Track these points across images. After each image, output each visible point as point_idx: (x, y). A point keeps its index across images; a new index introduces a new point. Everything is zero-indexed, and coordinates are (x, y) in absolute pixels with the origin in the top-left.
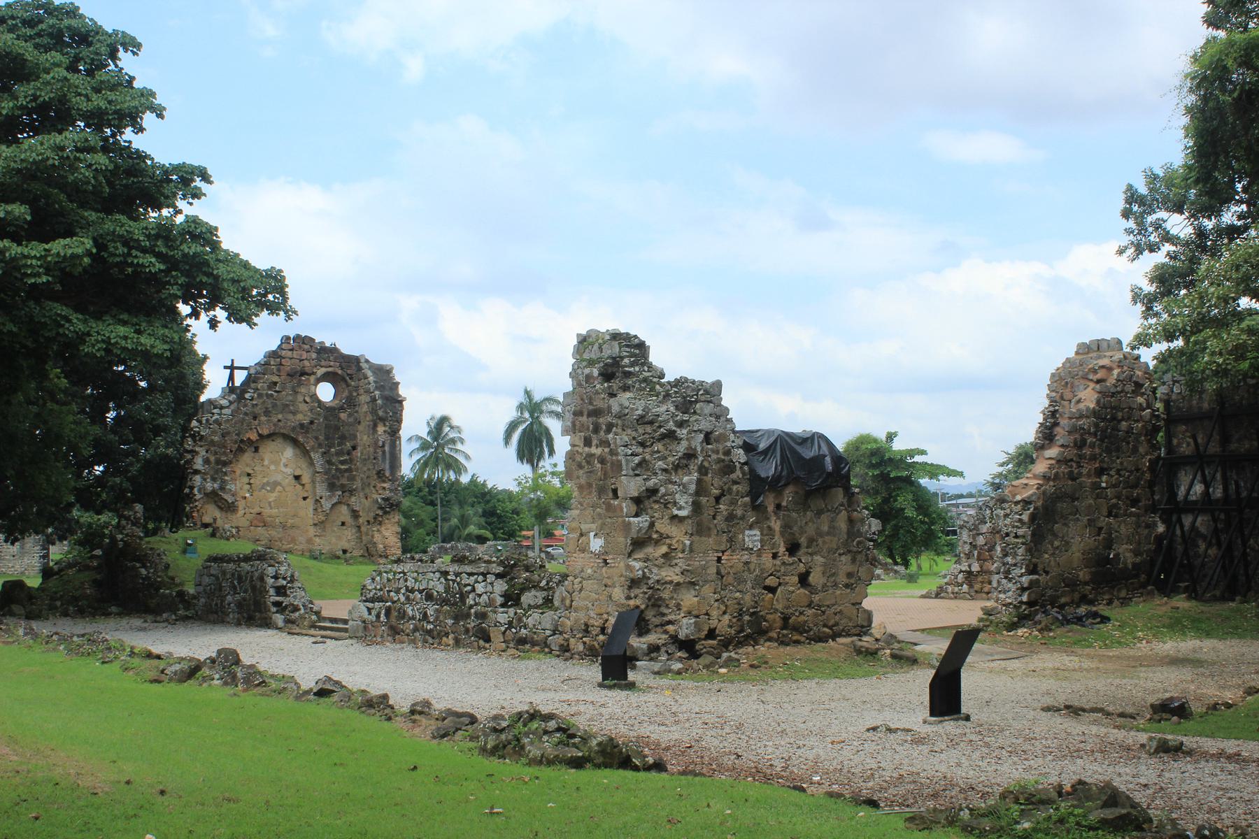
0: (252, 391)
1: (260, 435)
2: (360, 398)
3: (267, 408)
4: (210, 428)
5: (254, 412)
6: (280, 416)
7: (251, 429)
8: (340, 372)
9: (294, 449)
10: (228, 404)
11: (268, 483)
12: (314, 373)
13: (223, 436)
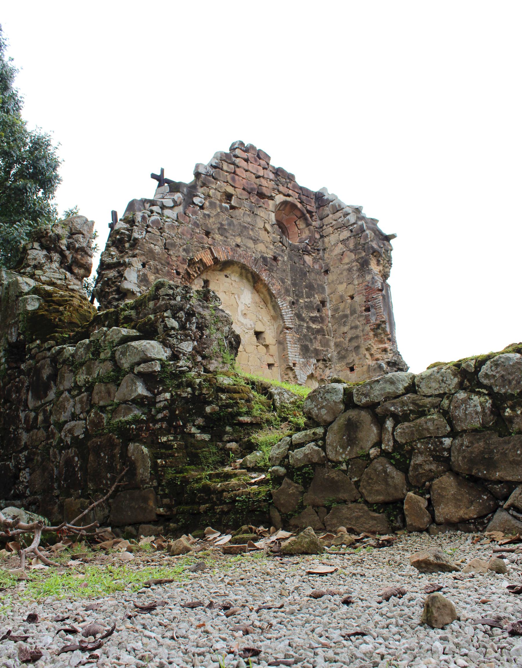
0: (202, 196)
2: (326, 240)
3: (222, 225)
4: (147, 232)
5: (205, 224)
6: (238, 240)
7: (203, 248)
8: (299, 205)
9: (252, 293)
10: (172, 204)
12: (271, 198)
13: (166, 247)
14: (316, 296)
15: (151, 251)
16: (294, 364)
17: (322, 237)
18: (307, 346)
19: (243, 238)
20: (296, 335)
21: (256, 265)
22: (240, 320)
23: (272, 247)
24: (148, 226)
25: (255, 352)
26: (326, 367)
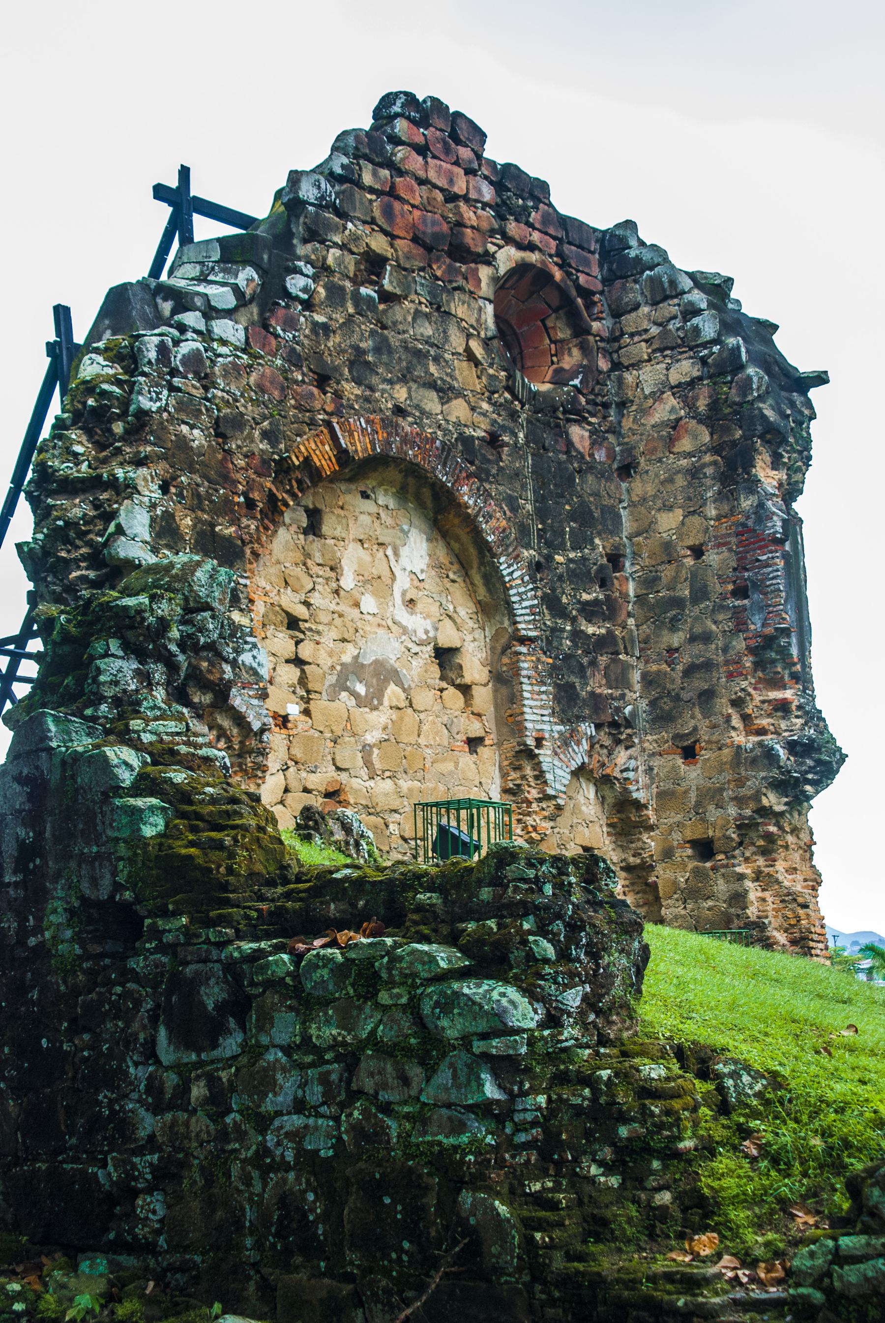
0: (309, 270)
1: (343, 456)
2: (629, 377)
4: (172, 389)
6: (401, 394)
7: (312, 423)
8: (558, 275)
9: (429, 540)
11: (356, 668)
12: (488, 259)
14: (597, 541)
15: (183, 443)
16: (539, 741)
17: (617, 366)
18: (572, 686)
19: (414, 386)
20: (544, 658)
21: (444, 466)
22: (398, 618)
23: (485, 406)
24: (174, 372)
25: (437, 707)
26: (618, 742)
